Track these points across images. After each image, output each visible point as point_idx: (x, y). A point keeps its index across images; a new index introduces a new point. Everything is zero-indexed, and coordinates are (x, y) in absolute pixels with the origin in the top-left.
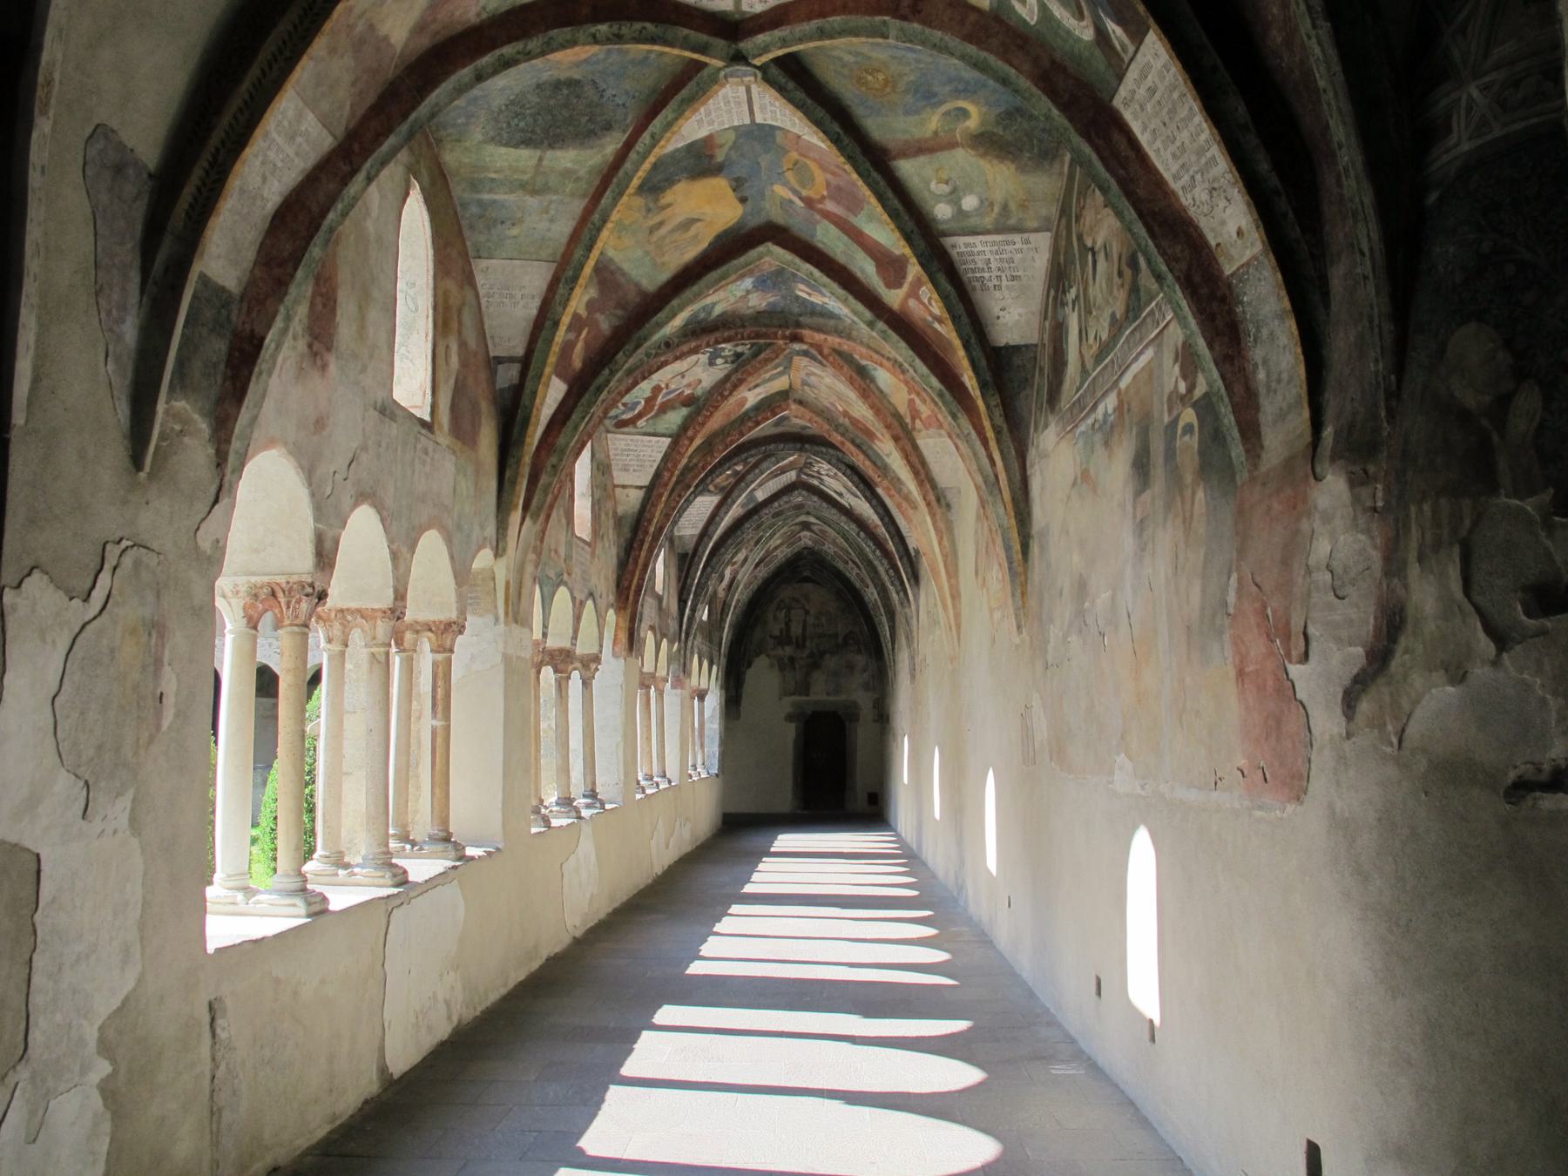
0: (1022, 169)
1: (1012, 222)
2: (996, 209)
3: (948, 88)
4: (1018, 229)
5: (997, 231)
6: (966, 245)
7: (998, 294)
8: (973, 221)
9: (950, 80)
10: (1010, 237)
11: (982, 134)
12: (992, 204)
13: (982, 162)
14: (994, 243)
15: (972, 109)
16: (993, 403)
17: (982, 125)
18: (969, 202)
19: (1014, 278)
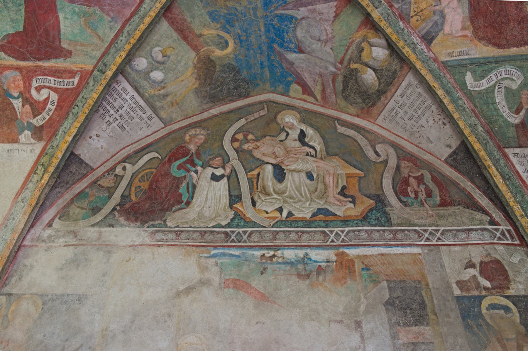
0: (197, 92)
1: (158, 104)
2: (162, 92)
4: (155, 110)
5: (146, 101)
6: (124, 89)
7: (104, 126)
8: (144, 83)
9: (245, 31)
10: (147, 108)
11: (212, 61)
12: (164, 88)
13: (190, 70)
14: (136, 103)
15: (230, 49)
16: (50, 183)
17: (219, 58)
18: (157, 75)
19: (122, 127)
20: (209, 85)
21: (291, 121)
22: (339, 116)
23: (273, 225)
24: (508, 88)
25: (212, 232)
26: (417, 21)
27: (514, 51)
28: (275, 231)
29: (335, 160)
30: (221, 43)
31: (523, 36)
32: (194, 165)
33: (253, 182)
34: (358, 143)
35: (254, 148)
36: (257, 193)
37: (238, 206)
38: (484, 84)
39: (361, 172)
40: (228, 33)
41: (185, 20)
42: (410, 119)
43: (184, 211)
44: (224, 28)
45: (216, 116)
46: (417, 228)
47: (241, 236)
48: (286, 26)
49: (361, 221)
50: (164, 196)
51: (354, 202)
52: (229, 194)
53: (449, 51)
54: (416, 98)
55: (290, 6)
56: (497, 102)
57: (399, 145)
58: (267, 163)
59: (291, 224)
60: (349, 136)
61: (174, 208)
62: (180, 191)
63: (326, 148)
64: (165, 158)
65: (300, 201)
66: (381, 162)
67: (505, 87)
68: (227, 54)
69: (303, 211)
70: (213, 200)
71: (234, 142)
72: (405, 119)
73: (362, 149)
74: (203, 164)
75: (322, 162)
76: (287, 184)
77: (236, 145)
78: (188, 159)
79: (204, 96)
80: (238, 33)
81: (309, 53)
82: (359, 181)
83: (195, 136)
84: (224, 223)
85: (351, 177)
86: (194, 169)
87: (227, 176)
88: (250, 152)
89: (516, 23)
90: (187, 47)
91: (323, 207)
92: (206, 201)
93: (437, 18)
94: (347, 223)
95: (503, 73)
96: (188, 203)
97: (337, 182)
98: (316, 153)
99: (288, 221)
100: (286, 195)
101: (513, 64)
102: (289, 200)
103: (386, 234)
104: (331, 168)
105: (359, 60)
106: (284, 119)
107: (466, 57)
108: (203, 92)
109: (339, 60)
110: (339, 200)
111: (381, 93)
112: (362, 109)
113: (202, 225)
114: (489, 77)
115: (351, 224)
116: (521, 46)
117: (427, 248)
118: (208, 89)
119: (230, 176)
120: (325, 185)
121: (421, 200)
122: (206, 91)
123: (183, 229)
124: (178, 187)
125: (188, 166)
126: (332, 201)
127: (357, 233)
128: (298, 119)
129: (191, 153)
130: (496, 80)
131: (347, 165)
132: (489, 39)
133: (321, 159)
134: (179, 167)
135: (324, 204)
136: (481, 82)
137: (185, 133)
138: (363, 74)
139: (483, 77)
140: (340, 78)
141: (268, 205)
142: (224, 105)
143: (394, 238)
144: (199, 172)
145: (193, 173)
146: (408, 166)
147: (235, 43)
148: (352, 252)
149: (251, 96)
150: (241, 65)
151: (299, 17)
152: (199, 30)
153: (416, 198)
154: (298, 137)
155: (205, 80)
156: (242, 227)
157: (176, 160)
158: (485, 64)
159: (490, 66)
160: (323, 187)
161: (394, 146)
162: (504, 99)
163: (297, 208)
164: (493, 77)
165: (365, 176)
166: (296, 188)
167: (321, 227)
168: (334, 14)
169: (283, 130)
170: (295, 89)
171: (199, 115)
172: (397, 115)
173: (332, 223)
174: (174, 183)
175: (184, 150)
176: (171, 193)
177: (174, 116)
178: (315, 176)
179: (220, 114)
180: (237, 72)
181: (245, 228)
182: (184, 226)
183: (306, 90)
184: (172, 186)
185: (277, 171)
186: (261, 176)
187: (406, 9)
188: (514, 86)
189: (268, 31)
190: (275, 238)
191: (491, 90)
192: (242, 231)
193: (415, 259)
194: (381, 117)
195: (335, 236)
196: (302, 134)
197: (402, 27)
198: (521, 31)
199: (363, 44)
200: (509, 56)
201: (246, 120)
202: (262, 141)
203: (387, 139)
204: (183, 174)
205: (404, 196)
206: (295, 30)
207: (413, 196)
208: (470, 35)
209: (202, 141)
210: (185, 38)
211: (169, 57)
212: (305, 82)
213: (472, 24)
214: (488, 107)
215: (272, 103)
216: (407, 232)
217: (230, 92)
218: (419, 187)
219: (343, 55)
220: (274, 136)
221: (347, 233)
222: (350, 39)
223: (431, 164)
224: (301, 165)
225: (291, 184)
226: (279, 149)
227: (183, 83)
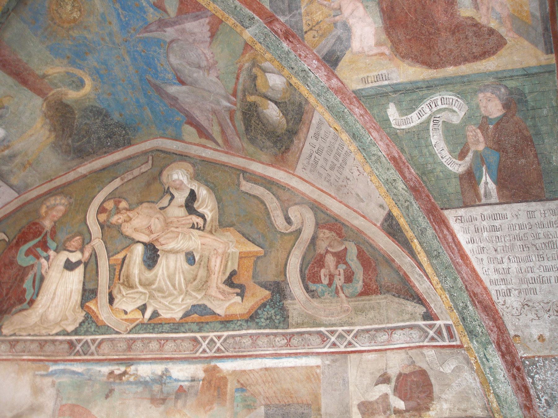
0: (55, 146)
2: (6, 152)
3: (95, 64)
11: (67, 106)
12: (8, 147)
17: (76, 101)
20: (70, 136)
21: (181, 178)
22: (247, 167)
23: (130, 331)
24: (448, 123)
25: (54, 342)
26: (314, 37)
27: (450, 71)
28: (131, 339)
29: (228, 233)
30: (73, 82)
31: (461, 50)
32: (46, 248)
33: (115, 270)
34: (265, 205)
35: (125, 221)
36: (117, 285)
37: (91, 305)
38: (414, 119)
39: (261, 249)
40: (80, 69)
41: (19, 60)
42: (332, 168)
43: (25, 313)
44: (72, 63)
45: (85, 176)
46: (322, 329)
47: (89, 346)
48: (155, 51)
49: (247, 321)
50: (4, 293)
51: (242, 295)
52: (83, 288)
53: (362, 76)
54: (333, 141)
55: (153, 27)
56: (433, 143)
57: (323, 206)
58: (139, 242)
59: (153, 329)
60: (254, 196)
61: (14, 310)
62: (24, 286)
63: (220, 215)
64: (13, 240)
65: (171, 295)
66: (291, 233)
67: (444, 122)
68: (86, 95)
69: (173, 310)
70: (62, 298)
71: (101, 213)
72: (327, 168)
73: (268, 214)
74: (57, 246)
75: (211, 236)
76: (158, 271)
77: (103, 217)
78: (39, 241)
79: (66, 152)
80: (95, 68)
81: (191, 84)
82: (255, 263)
83: (55, 206)
84: (70, 329)
85: (245, 257)
86: (45, 254)
87: (85, 263)
88: (118, 227)
89: (448, 33)
90: (29, 93)
91: (200, 303)
92: (53, 299)
93: (339, 32)
94: (228, 325)
95: (439, 103)
96: (32, 302)
97: (226, 266)
98: (204, 224)
99: (150, 324)
100: (154, 287)
101: (452, 89)
102: (157, 294)
103: (277, 339)
104: (221, 246)
105: (255, 90)
106: (172, 175)
107: (386, 83)
108: (64, 146)
109: (231, 92)
110: (223, 293)
111: (292, 133)
112: (276, 155)
113: (44, 332)
114: (420, 109)
115: (233, 326)
116: (460, 64)
117: (330, 358)
118: (70, 141)
119: (88, 262)
120: (208, 270)
121: (337, 287)
122: (68, 145)
123: (21, 338)
124: (22, 280)
125: (39, 250)
126: (213, 294)
127: (238, 339)
128: (191, 174)
129: (45, 231)
130: (430, 113)
131: (243, 239)
132: (415, 56)
133: (211, 232)
134: (29, 252)
135: (202, 298)
136: (409, 116)
137: (42, 203)
138: (265, 109)
139: (412, 110)
140: (239, 115)
141: (128, 303)
142: (96, 160)
143: (288, 345)
144: (51, 257)
145: (43, 260)
146: (327, 238)
147: (94, 80)
148: (226, 366)
149: (133, 145)
150: (109, 106)
151: (168, 40)
152: (41, 70)
153: (330, 284)
154: (186, 201)
155: (63, 130)
156: (92, 334)
157: (26, 242)
158: (413, 91)
159: (421, 93)
160: (205, 274)
161: (316, 208)
162: (442, 138)
163: (166, 306)
164: (425, 109)
165: (265, 256)
166: (169, 277)
167: (192, 332)
168: (209, 34)
169: (167, 192)
170: (189, 131)
171: (64, 177)
172: (316, 163)
173: (207, 326)
174: (18, 275)
175: (36, 228)
176: (13, 288)
177: (29, 181)
178: (197, 259)
179: (90, 173)
180: (106, 116)
181: (95, 335)
182: (22, 333)
183: (202, 132)
184: (16, 280)
185: (149, 253)
186: (126, 261)
187: (296, 22)
188: (456, 120)
189: (134, 59)
190: (129, 348)
191: (424, 128)
192: (91, 340)
193: (310, 375)
194: (300, 166)
195: (208, 344)
196: (192, 196)
197: (287, 49)
198: (457, 43)
199: (254, 70)
200: (445, 79)
201: (122, 179)
202: (136, 210)
203: (308, 197)
204: (31, 263)
205: (314, 282)
206: (167, 56)
207: (325, 281)
208: (387, 52)
209: (60, 214)
210: (24, 82)
211: (7, 108)
212: (198, 122)
213: (389, 37)
214: (421, 152)
215: (159, 153)
216: (307, 336)
217: (101, 142)
218: (337, 267)
219: (234, 86)
220: (153, 202)
221: (225, 340)
222: (237, 63)
223: (361, 232)
224: (181, 242)
225: (163, 271)
226: (157, 220)
227: (33, 138)
